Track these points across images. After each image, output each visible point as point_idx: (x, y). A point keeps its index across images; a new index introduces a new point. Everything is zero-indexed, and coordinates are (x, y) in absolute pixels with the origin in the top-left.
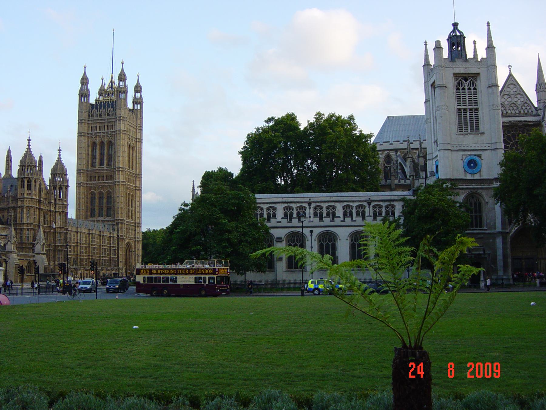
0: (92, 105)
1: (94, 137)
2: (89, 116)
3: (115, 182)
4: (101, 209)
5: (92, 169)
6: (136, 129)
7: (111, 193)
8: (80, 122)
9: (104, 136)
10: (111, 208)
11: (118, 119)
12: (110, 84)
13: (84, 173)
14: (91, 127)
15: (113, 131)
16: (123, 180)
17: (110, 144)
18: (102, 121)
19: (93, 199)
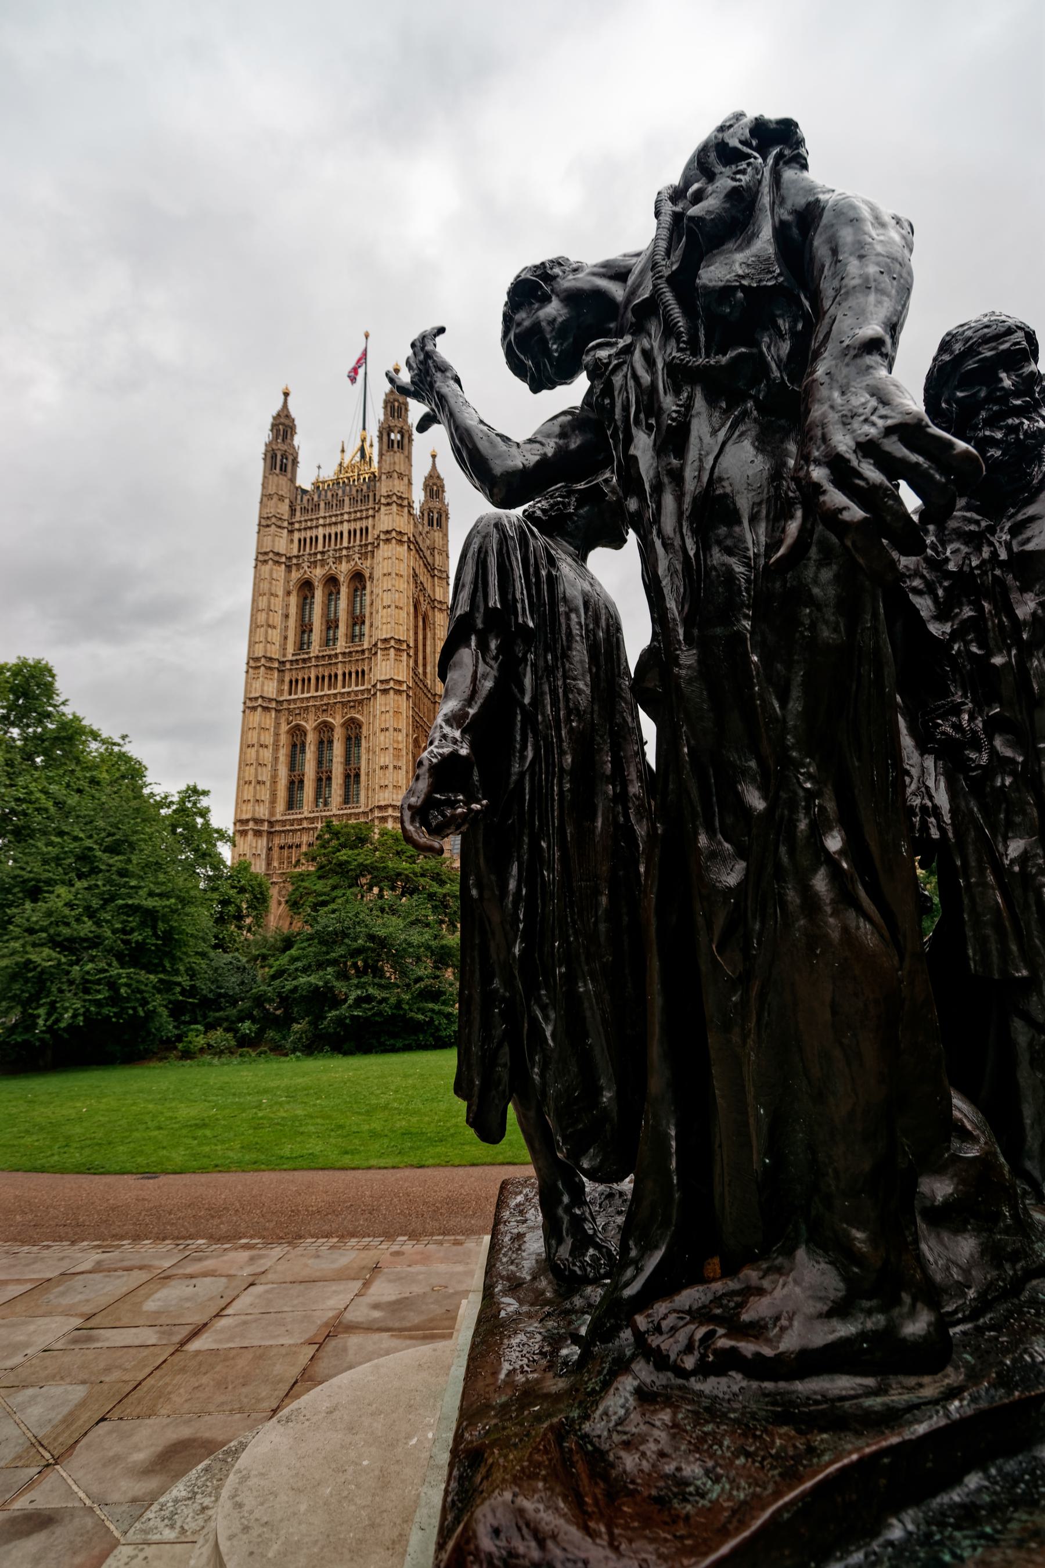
0: (304, 492)
1: (305, 565)
2: (293, 511)
3: (374, 686)
4: (323, 780)
5: (298, 657)
6: (433, 576)
7: (359, 725)
8: (265, 523)
9: (338, 560)
10: (358, 775)
11: (383, 501)
12: (359, 455)
13: (271, 669)
14: (300, 540)
15: (370, 540)
16: (400, 678)
17: (358, 579)
18: (334, 519)
19: (297, 748)
